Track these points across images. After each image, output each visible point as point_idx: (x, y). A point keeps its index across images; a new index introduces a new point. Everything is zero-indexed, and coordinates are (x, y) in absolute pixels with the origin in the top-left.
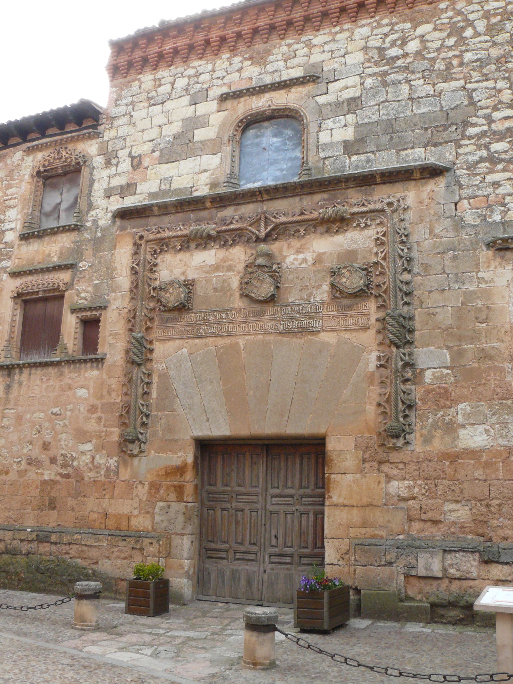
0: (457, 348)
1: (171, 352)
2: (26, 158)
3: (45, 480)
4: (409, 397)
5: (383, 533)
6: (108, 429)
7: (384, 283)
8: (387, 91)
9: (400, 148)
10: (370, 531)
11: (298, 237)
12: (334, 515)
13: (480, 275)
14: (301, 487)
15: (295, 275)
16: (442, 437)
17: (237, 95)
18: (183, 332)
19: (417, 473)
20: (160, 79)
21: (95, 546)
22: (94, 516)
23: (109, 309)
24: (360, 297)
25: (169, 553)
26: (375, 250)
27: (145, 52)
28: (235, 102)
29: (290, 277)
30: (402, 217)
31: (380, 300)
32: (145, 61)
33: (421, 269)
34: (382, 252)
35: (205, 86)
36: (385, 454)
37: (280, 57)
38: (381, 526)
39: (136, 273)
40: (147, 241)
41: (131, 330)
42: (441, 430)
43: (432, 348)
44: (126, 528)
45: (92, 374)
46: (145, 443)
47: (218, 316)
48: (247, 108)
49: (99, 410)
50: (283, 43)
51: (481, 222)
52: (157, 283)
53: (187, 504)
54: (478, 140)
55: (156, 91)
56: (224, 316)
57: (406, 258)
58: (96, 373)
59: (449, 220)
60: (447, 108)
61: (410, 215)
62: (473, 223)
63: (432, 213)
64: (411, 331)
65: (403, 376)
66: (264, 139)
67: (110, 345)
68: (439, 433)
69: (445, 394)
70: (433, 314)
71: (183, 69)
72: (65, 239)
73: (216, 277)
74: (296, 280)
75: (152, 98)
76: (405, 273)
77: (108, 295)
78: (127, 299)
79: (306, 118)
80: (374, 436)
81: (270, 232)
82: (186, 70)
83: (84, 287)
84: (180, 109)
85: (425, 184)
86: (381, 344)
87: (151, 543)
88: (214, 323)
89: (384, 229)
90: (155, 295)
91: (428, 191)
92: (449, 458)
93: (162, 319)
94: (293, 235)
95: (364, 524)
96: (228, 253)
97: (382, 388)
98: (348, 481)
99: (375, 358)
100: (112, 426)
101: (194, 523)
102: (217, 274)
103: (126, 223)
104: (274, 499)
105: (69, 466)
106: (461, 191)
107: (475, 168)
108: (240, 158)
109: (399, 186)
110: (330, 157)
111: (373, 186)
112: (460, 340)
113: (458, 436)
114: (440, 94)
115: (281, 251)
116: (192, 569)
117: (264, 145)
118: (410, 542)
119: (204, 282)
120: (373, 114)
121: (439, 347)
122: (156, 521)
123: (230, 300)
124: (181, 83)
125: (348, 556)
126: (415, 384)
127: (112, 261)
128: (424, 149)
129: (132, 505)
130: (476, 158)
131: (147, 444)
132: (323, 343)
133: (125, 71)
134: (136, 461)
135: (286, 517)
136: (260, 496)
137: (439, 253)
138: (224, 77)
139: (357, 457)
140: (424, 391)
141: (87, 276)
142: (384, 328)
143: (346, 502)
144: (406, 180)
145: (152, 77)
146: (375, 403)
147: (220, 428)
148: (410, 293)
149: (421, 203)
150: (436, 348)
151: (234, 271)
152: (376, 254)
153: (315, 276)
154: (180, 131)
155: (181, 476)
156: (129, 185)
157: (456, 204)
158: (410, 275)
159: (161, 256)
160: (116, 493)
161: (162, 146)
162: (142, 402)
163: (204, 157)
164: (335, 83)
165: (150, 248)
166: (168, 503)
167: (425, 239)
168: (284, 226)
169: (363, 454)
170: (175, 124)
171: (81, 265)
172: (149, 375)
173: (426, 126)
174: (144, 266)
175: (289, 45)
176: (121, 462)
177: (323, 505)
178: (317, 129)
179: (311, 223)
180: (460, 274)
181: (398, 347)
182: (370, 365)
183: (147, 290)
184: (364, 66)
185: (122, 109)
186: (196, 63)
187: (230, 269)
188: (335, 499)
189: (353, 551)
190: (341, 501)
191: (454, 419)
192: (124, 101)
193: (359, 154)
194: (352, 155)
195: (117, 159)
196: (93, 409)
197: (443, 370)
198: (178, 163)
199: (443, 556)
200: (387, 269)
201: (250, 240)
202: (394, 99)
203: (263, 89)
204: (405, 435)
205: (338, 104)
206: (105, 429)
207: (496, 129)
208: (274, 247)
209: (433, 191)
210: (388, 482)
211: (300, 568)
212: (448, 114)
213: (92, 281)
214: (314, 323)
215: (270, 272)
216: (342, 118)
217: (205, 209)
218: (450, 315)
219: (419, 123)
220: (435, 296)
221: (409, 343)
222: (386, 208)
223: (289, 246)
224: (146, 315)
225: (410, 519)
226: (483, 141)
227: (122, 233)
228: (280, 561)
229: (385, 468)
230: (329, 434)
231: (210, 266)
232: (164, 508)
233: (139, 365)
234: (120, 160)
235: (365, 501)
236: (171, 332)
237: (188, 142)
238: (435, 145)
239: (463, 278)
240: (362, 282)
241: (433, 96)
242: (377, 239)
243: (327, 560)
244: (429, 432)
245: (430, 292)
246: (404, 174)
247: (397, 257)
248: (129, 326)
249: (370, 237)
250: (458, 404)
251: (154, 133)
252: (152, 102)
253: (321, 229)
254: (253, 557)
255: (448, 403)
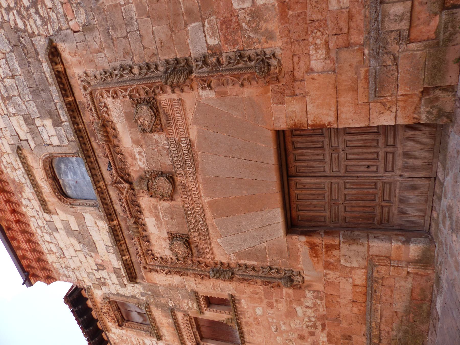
0: (185, 17)
1: (222, 250)
2: (113, 332)
3: (328, 341)
4: (233, 58)
5: (363, 70)
6: (284, 296)
7: (144, 89)
8: (13, 96)
9: (47, 83)
10: (361, 84)
11: (124, 158)
12: (346, 119)
13: (122, 3)
14: (322, 148)
15: (151, 161)
16: (266, 21)
17: (43, 203)
18: (205, 242)
19: (301, 43)
20: (49, 251)
21: (381, 312)
22: (355, 310)
23: (197, 290)
24: (158, 108)
25: (386, 257)
26: (121, 98)
27: (32, 260)
28: (49, 204)
29: (154, 164)
30: (93, 77)
31: (157, 91)
32: (39, 260)
33: (127, 57)
34: (122, 92)
35: (45, 222)
36: (286, 76)
37: (14, 174)
38: (356, 73)
39: (170, 272)
40: (147, 264)
41: (209, 278)
42: (259, 23)
43: (189, 41)
44: (364, 288)
45: (244, 304)
46: (292, 271)
47: (190, 217)
48: (50, 195)
49: (270, 301)
50: (5, 172)
51: (82, 7)
52: (174, 258)
53: (341, 242)
54: (24, 18)
55: (56, 253)
56: (189, 212)
57: (122, 71)
58: (243, 301)
59: (86, 36)
60: (10, 47)
61: (91, 71)
62: (85, 15)
63: (85, 52)
64: (177, 61)
65: (216, 65)
66: (70, 182)
67: (222, 291)
68: (263, 25)
69: (226, 23)
70: (161, 43)
71: (39, 237)
72: (157, 314)
73: (163, 218)
74: (155, 160)
75: (60, 256)
76: (133, 71)
77: (187, 290)
78: (189, 278)
79: (46, 155)
80: (271, 87)
81: (124, 180)
82: (38, 234)
83: (185, 305)
84: (62, 238)
85: (66, 60)
86: (192, 88)
87: (377, 271)
88: (196, 219)
89: (104, 91)
90: (182, 260)
91: (70, 57)
92: (285, 11)
93: (198, 255)
94: (124, 162)
95: (354, 90)
96: (145, 209)
97: (228, 84)
98: (313, 108)
99: (204, 92)
100: (282, 293)
101: (358, 235)
102: (161, 217)
103: (138, 275)
104: (334, 170)
105: (315, 324)
106: (63, 28)
107: (45, 17)
108: (86, 199)
109: (72, 82)
110: (67, 136)
111: (78, 103)
112: (178, 15)
113: (265, 5)
114: (3, 53)
115: (136, 171)
116: (400, 237)
117: (74, 183)
118: (372, 41)
119: (168, 226)
120: (31, 105)
121: (187, 34)
122: (357, 266)
123: (178, 208)
124: (47, 238)
125: (387, 103)
126: (221, 54)
127: (165, 286)
128: (43, 63)
129: (345, 283)
130: (37, 17)
131: (293, 269)
132: (198, 137)
133: (48, 272)
134: (306, 278)
135: (350, 159)
136: (332, 181)
137: (113, 43)
138: (37, 211)
139: (291, 102)
140: (226, 44)
141: (178, 302)
142: (179, 86)
143: (334, 109)
144: (67, 76)
145: (48, 255)
146: (241, 89)
147: (277, 216)
148: (147, 66)
149: (80, 63)
150: (188, 37)
151: (157, 205)
152: (124, 97)
153: (149, 145)
154: (75, 239)
155: (317, 246)
156: (115, 273)
157: (75, 32)
158: (135, 67)
159: (156, 254)
160: (335, 294)
161: (87, 251)
162: (261, 272)
163: (88, 224)
164: (20, 135)
165: (151, 262)
166: (341, 256)
167: (105, 56)
168: (118, 170)
169: (288, 96)
170: (72, 242)
171: (171, 305)
172: (240, 266)
173: (27, 63)
174: (163, 267)
175: (5, 167)
176: (310, 289)
177: (337, 129)
178: (51, 147)
179: (112, 150)
180: (126, 22)
181: (191, 72)
182: (210, 96)
183: (179, 265)
184: (3, 114)
185: (71, 274)
186: (33, 228)
187: (156, 208)
188: (331, 119)
189: (382, 98)
190: (332, 113)
191: (248, 11)
192: (66, 273)
193: (59, 115)
194: (61, 120)
195: (102, 279)
196: (270, 305)
197: (206, 28)
198: (95, 241)
199: (387, 3)
200: (133, 87)
201: (134, 193)
202: (17, 90)
203: (35, 185)
204: (267, 58)
205: (32, 132)
206: (284, 298)
207: (13, 3)
208: (134, 176)
209: (70, 53)
210: (312, 70)
211: (398, 145)
212: (14, 46)
213: (179, 299)
214: (184, 145)
215: (152, 180)
216: (39, 128)
217: (119, 224)
218: (159, 27)
219: (26, 69)
220: (146, 42)
221: (187, 61)
222: (88, 92)
223: (132, 165)
224: (197, 267)
225: (348, 45)
226: (24, 13)
227: (145, 278)
228: (391, 163)
229: (299, 74)
230: (272, 128)
231: (157, 221)
232: (345, 260)
233: (233, 273)
234: (101, 276)
235: (332, 91)
236: (206, 250)
237: (80, 234)
238: (38, 54)
239: (127, 18)
240: (145, 107)
241: (6, 58)
242: (114, 98)
243: (392, 123)
244: (262, 35)
245: (144, 48)
246: (61, 78)
247: (122, 79)
248: (206, 278)
249: (113, 102)
250: (234, 10)
251: (81, 255)
252: (62, 256)
253: (115, 142)
254: (387, 186)
255: (234, 20)
